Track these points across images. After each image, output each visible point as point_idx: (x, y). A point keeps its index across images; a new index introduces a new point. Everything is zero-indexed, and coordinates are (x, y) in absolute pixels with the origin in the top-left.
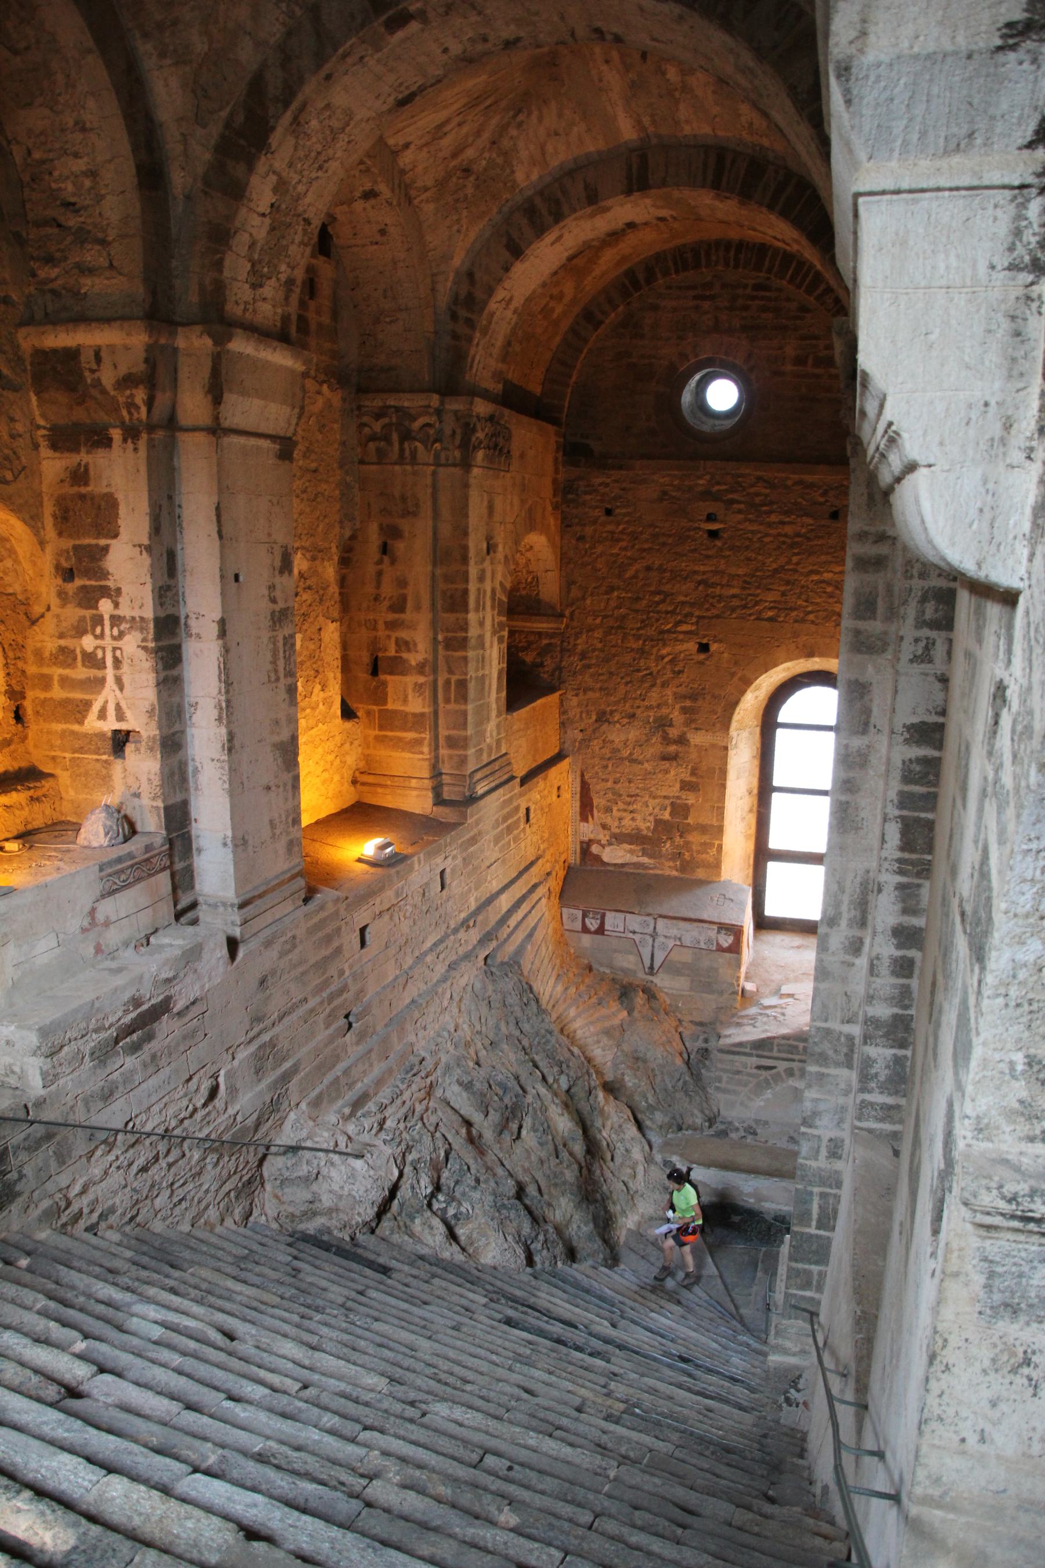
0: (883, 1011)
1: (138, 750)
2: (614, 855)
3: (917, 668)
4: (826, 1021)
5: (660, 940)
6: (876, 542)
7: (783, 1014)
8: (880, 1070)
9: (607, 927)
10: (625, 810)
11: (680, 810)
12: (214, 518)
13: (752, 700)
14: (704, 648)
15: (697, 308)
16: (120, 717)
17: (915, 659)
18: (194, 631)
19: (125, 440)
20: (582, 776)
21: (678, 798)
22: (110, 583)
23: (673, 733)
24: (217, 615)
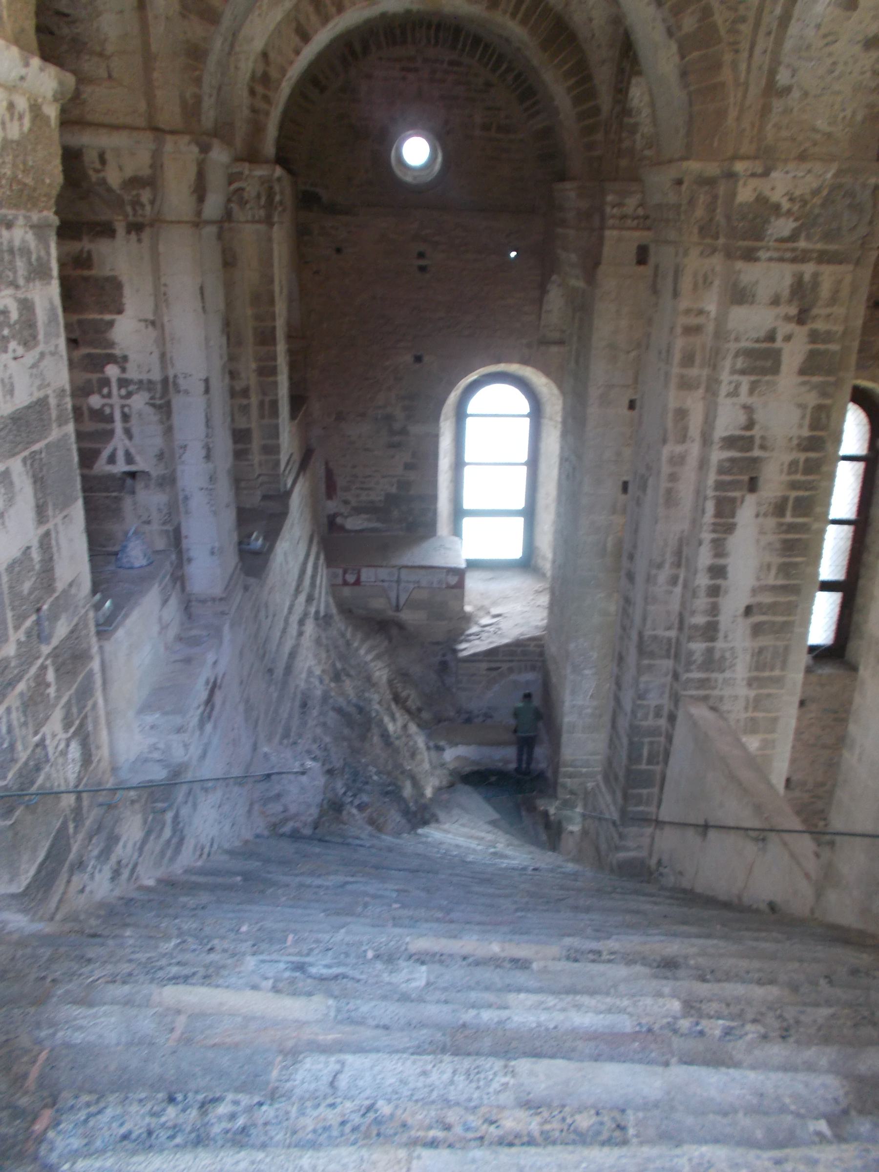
0: (700, 620)
1: (147, 487)
2: (353, 523)
3: (729, 401)
4: (654, 630)
5: (403, 585)
6: (697, 315)
7: (499, 629)
8: (698, 657)
10: (362, 489)
11: (404, 485)
12: (199, 297)
13: (453, 397)
14: (418, 359)
15: (404, 78)
16: (129, 459)
17: (729, 395)
18: (182, 388)
19: (129, 232)
20: (327, 464)
22: (117, 351)
23: (397, 426)
24: (203, 376)
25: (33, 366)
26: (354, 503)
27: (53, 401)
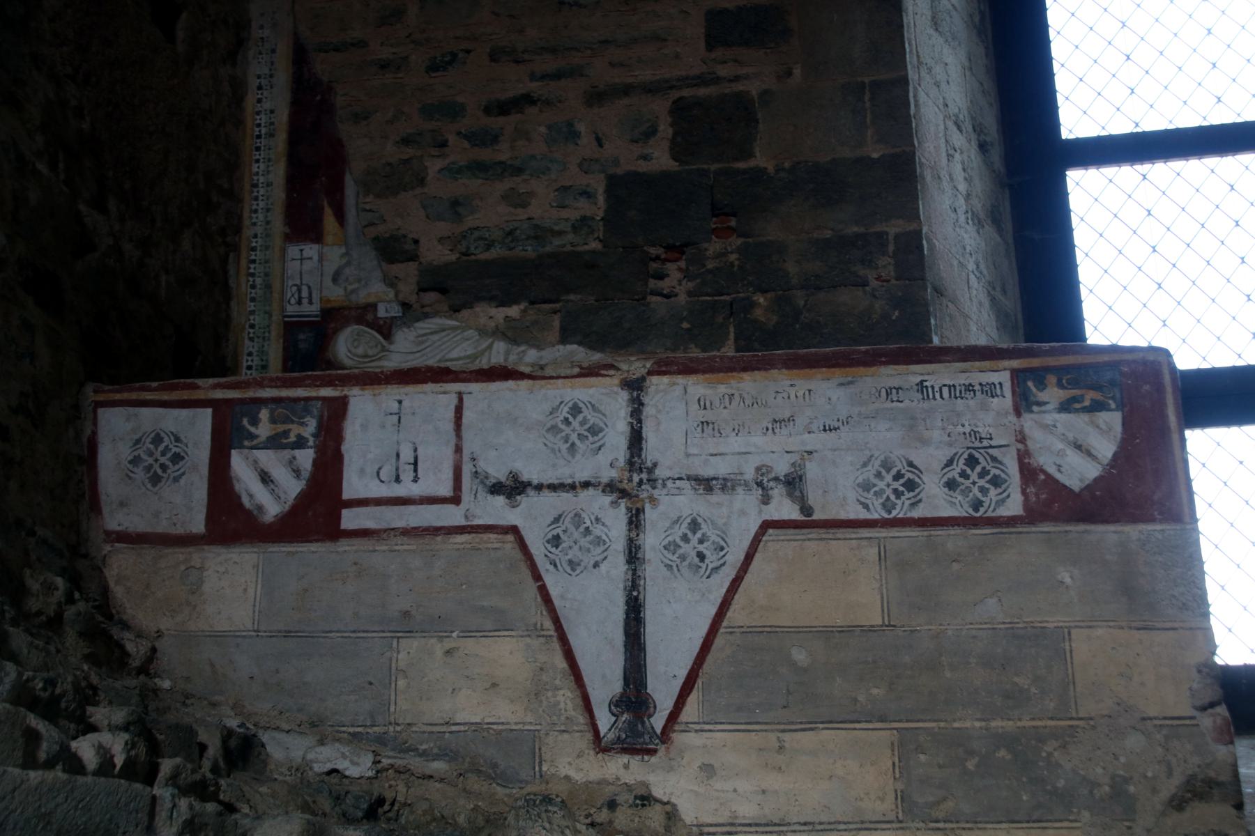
5: (669, 509)
9: (355, 484)
10: (478, 168)
20: (300, 57)
21: (701, 80)
26: (436, 253)
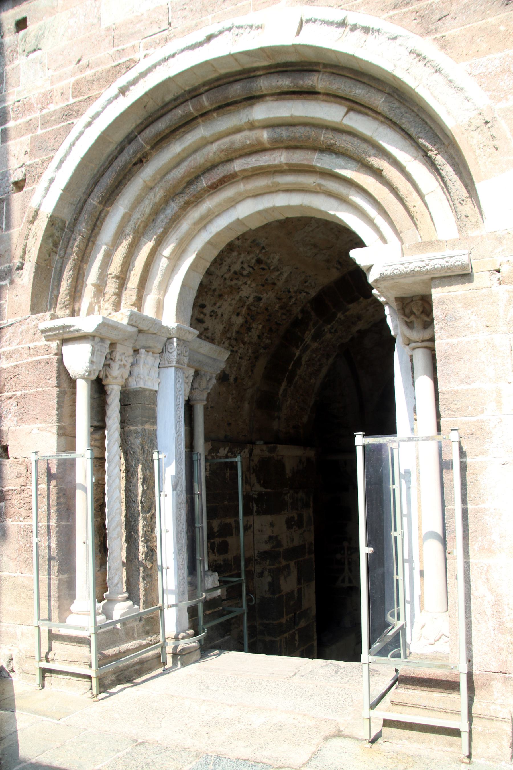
25: (301, 534)
27: (307, 546)
